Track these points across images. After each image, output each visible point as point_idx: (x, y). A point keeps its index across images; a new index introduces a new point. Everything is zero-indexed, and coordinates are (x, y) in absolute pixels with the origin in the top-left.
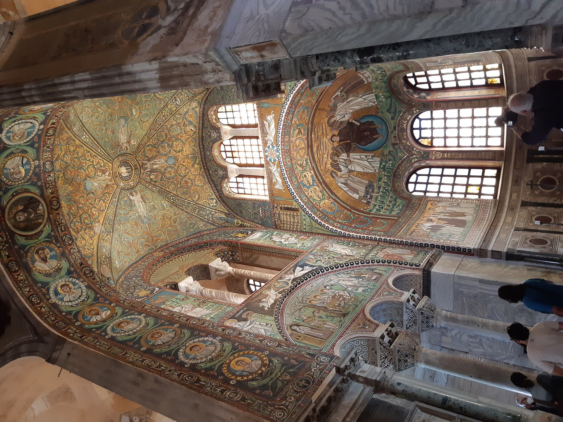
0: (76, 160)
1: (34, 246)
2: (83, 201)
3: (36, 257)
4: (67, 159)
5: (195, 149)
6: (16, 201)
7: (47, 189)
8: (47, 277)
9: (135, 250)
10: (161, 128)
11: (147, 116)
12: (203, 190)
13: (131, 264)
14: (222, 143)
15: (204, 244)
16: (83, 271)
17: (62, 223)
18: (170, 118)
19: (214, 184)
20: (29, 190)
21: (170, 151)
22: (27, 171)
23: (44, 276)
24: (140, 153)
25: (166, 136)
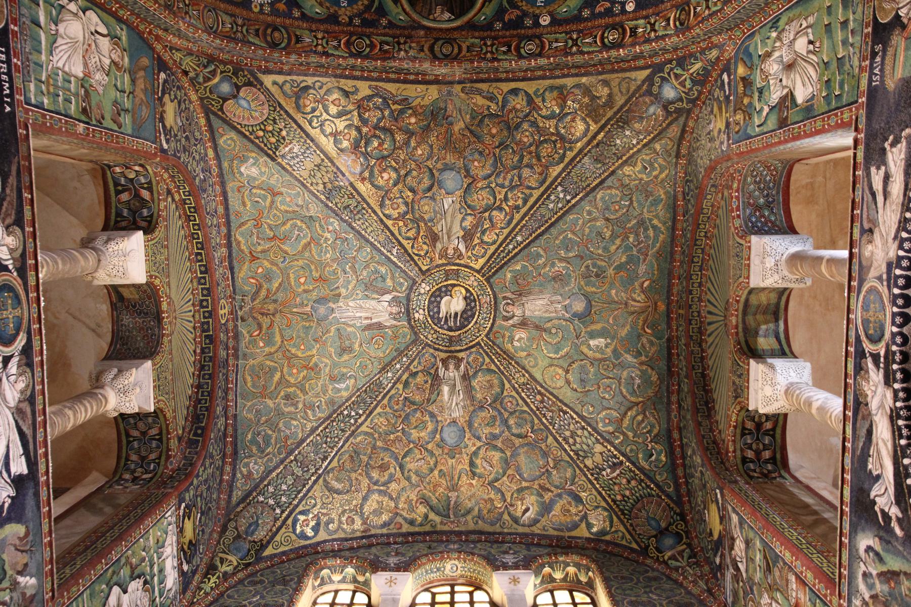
0: (516, 159)
2: (420, 152)
4: (525, 136)
5: (469, 517)
7: (483, 39)
9: (259, 248)
10: (543, 423)
11: (582, 380)
12: (351, 511)
13: (232, 217)
14: (479, 588)
15: (203, 428)
16: (283, 30)
17: (400, 50)
18: (565, 450)
19: (359, 547)
21: (479, 438)
24: (487, 360)
25: (519, 436)
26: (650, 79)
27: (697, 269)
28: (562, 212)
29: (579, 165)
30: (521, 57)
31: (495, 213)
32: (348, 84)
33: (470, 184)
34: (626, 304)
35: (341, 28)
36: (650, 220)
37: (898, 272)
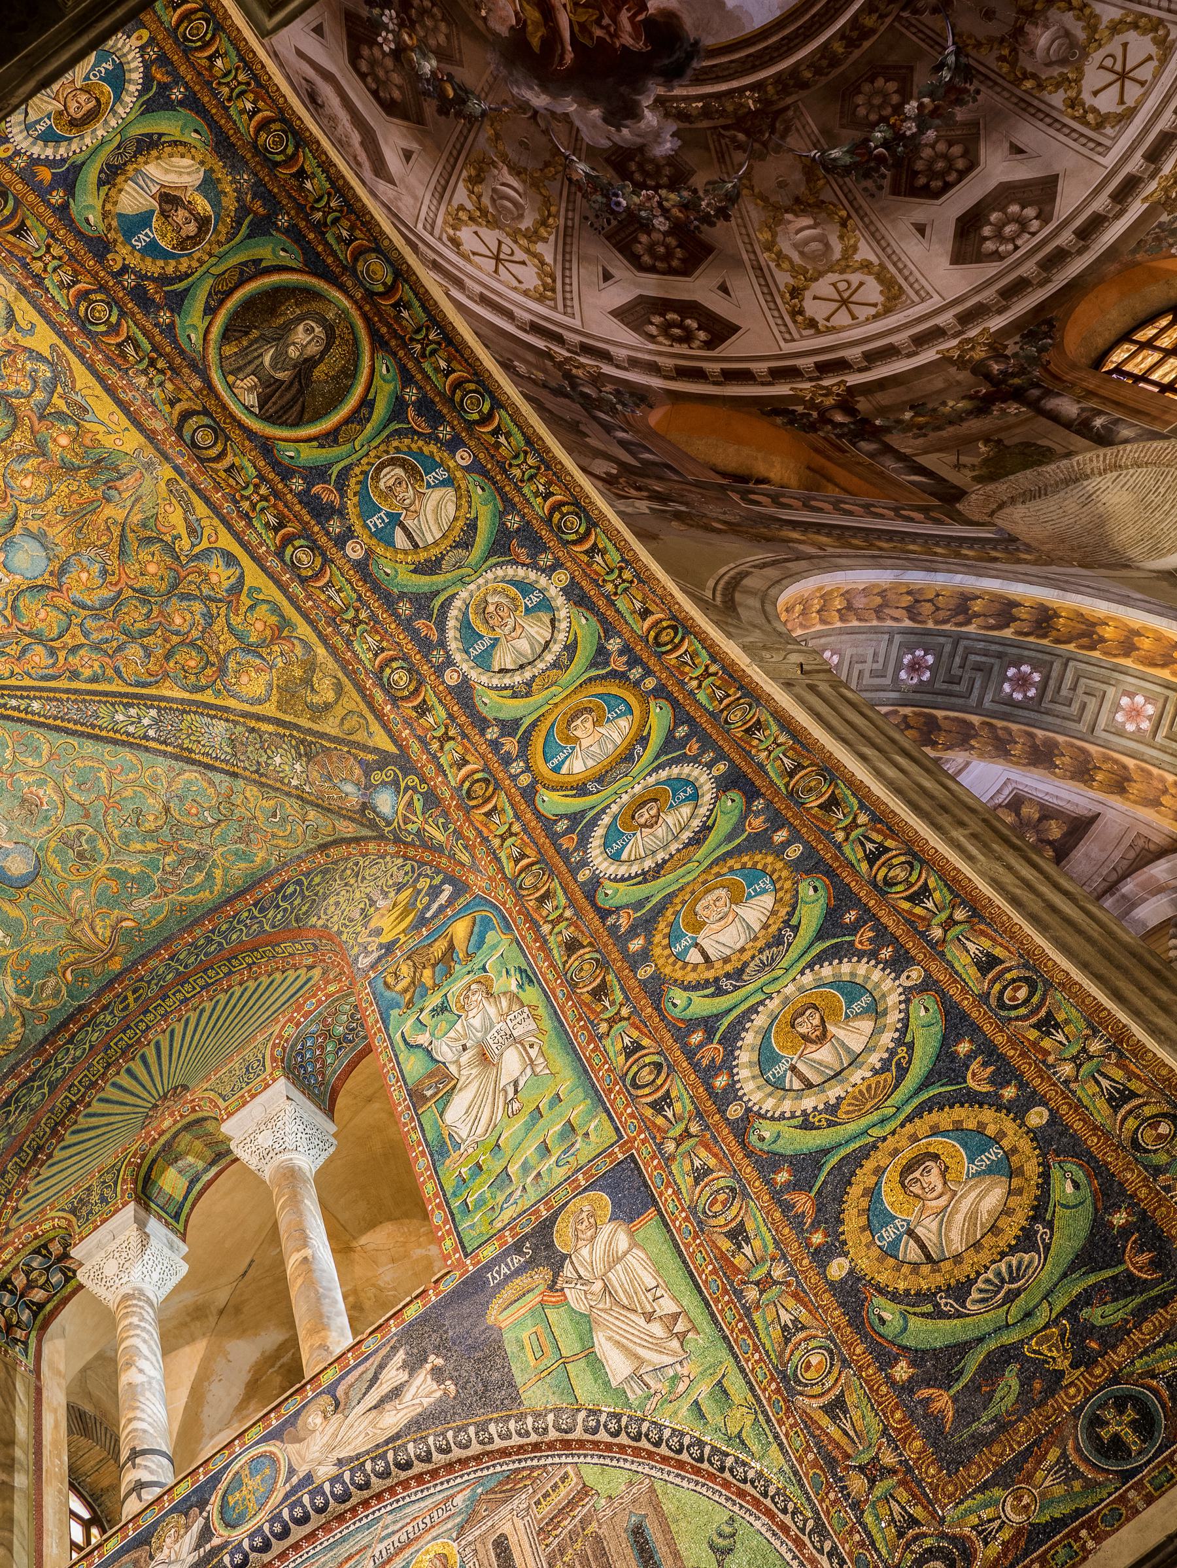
1: (220, 244)
2: (27, 483)
3: (203, 205)
6: (348, 389)
7: (262, 477)
8: (150, 135)
16: (11, 203)
17: (145, 372)
20: (322, 446)
22: (368, 508)
23: (161, 135)
26: (385, 760)
27: (201, 982)
28: (124, 738)
29: (207, 720)
30: (280, 554)
31: (39, 649)
32: (25, 312)
33: (48, 587)
34: (77, 921)
35: (98, 267)
36: (214, 865)
37: (306, 1499)
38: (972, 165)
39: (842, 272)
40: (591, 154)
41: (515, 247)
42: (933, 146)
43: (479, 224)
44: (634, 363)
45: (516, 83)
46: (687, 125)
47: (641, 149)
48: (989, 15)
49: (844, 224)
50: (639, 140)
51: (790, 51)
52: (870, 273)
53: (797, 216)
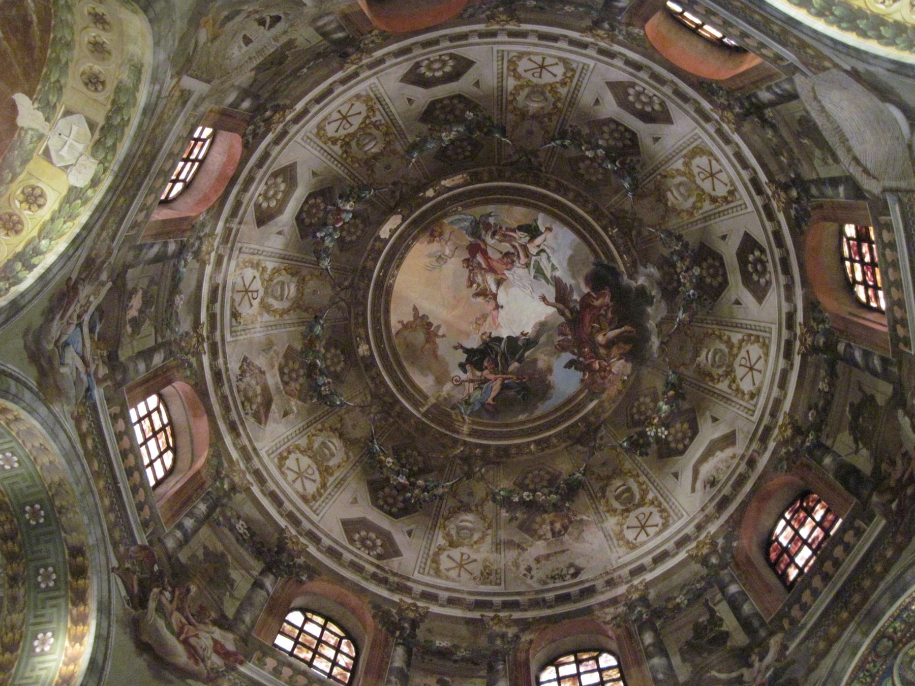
38: (611, 120)
39: (694, 176)
40: (672, 310)
41: (740, 356)
42: (607, 140)
43: (735, 376)
44: (789, 298)
45: (652, 355)
46: (638, 262)
47: (659, 284)
48: (530, 133)
49: (665, 177)
50: (655, 284)
51: (582, 217)
52: (690, 162)
53: (667, 200)
